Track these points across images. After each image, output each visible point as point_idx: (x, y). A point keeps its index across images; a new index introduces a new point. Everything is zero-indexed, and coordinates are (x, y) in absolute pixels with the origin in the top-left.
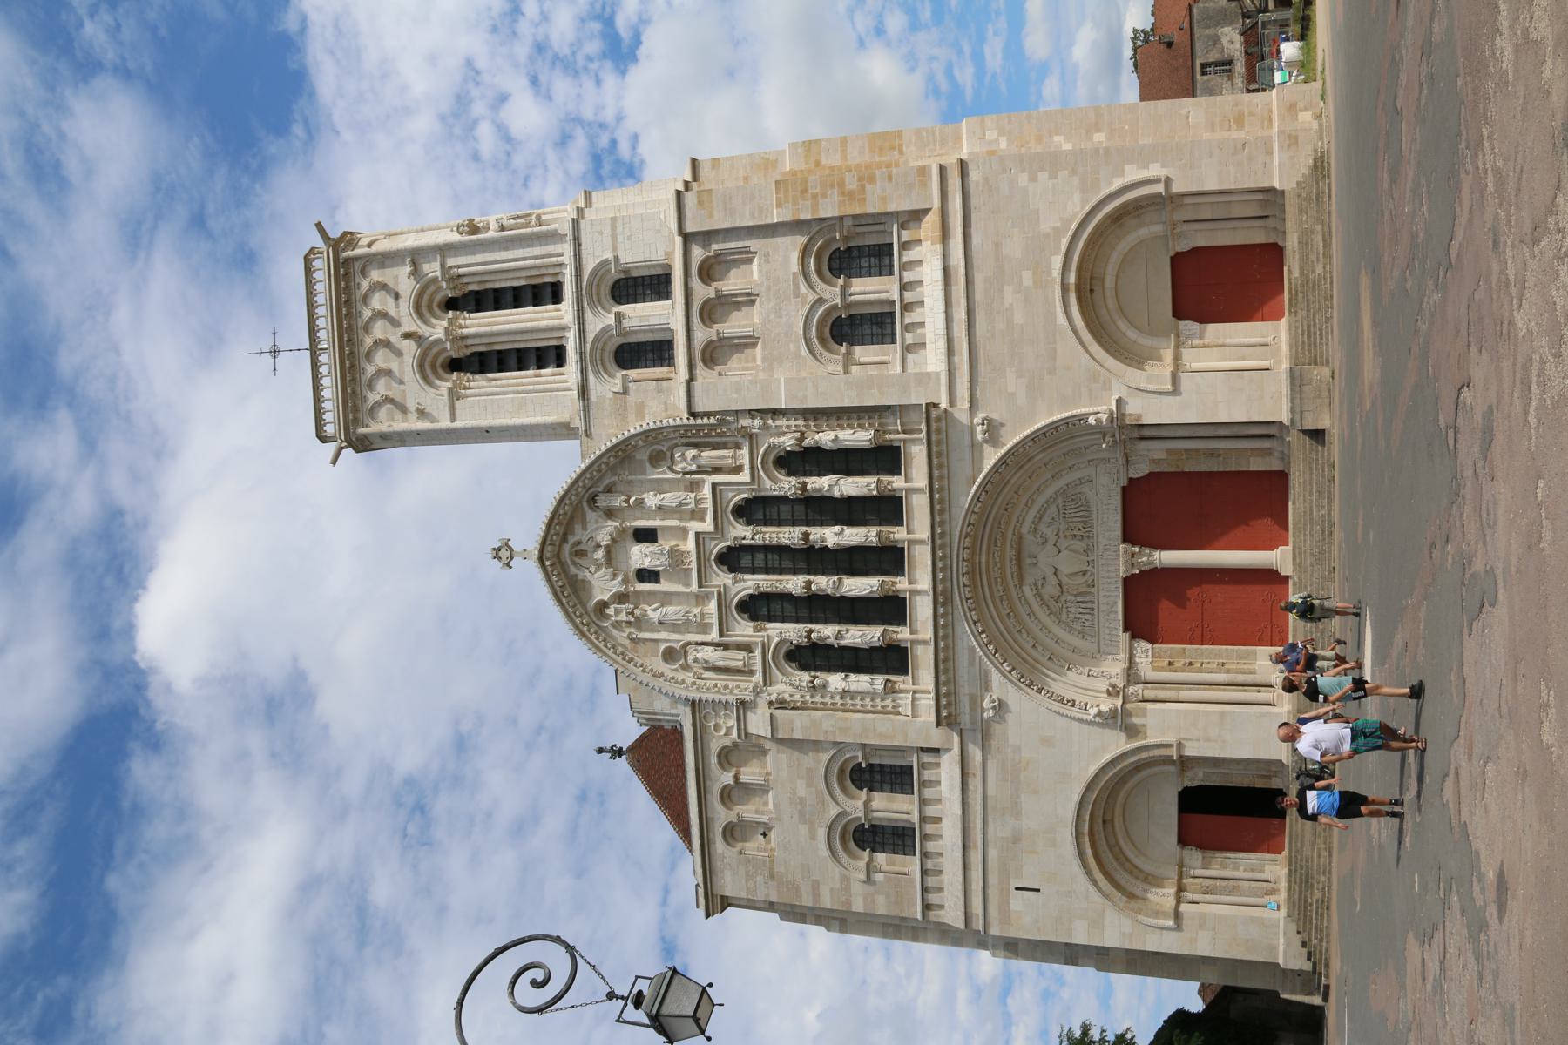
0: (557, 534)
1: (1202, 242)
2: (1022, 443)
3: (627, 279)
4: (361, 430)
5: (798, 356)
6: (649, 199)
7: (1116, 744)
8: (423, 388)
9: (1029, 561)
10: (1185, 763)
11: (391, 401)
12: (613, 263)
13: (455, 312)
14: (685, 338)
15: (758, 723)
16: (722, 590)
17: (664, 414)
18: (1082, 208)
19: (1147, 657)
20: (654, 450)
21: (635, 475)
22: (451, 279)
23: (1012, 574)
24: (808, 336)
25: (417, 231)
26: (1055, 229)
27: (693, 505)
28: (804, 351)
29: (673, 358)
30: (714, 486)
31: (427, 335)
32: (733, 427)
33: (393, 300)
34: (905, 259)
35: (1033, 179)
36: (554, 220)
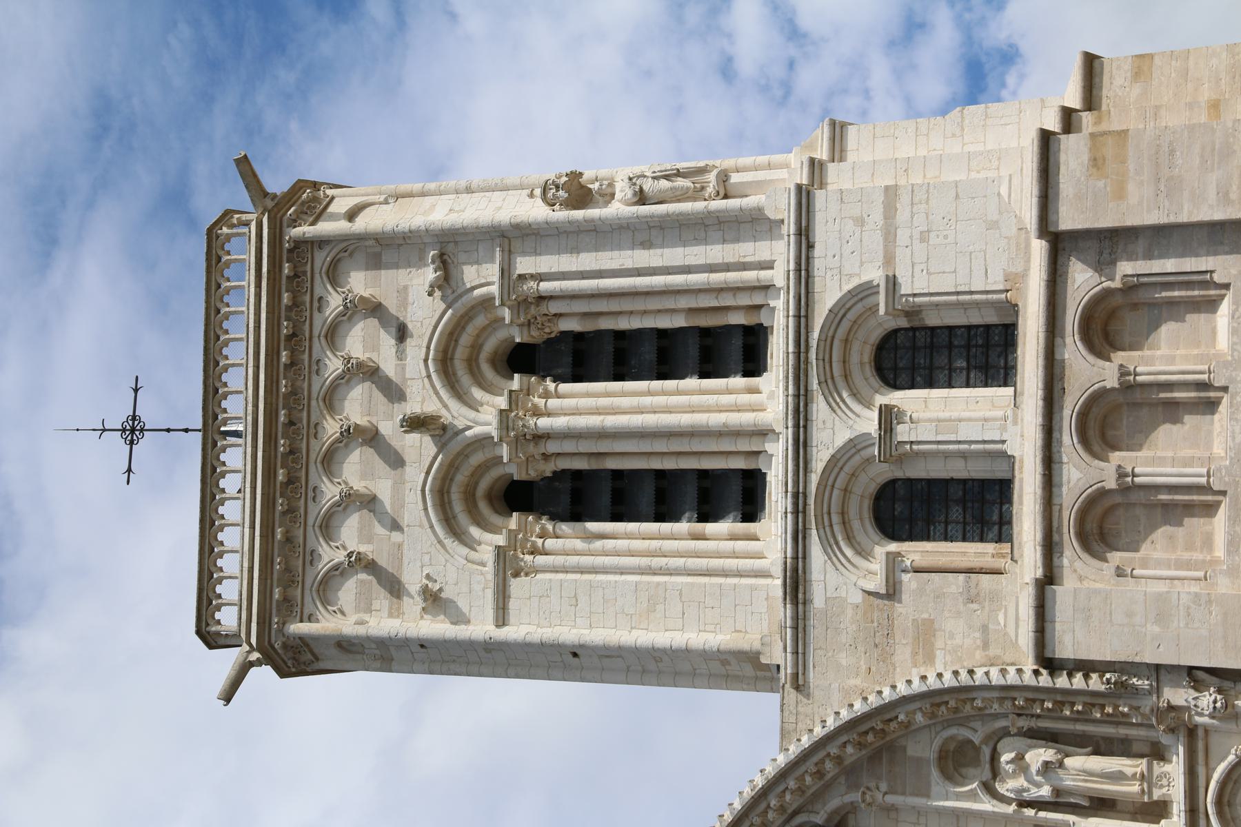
3: (913, 329)
4: (298, 628)
6: (980, 147)
8: (440, 542)
11: (371, 566)
12: (882, 298)
13: (525, 378)
14: (1039, 478)
17: (979, 655)
20: (952, 738)
21: (903, 794)
22: (522, 304)
25: (457, 192)
29: (1010, 523)
31: (460, 424)
32: (1147, 704)
33: (393, 342)
36: (758, 186)
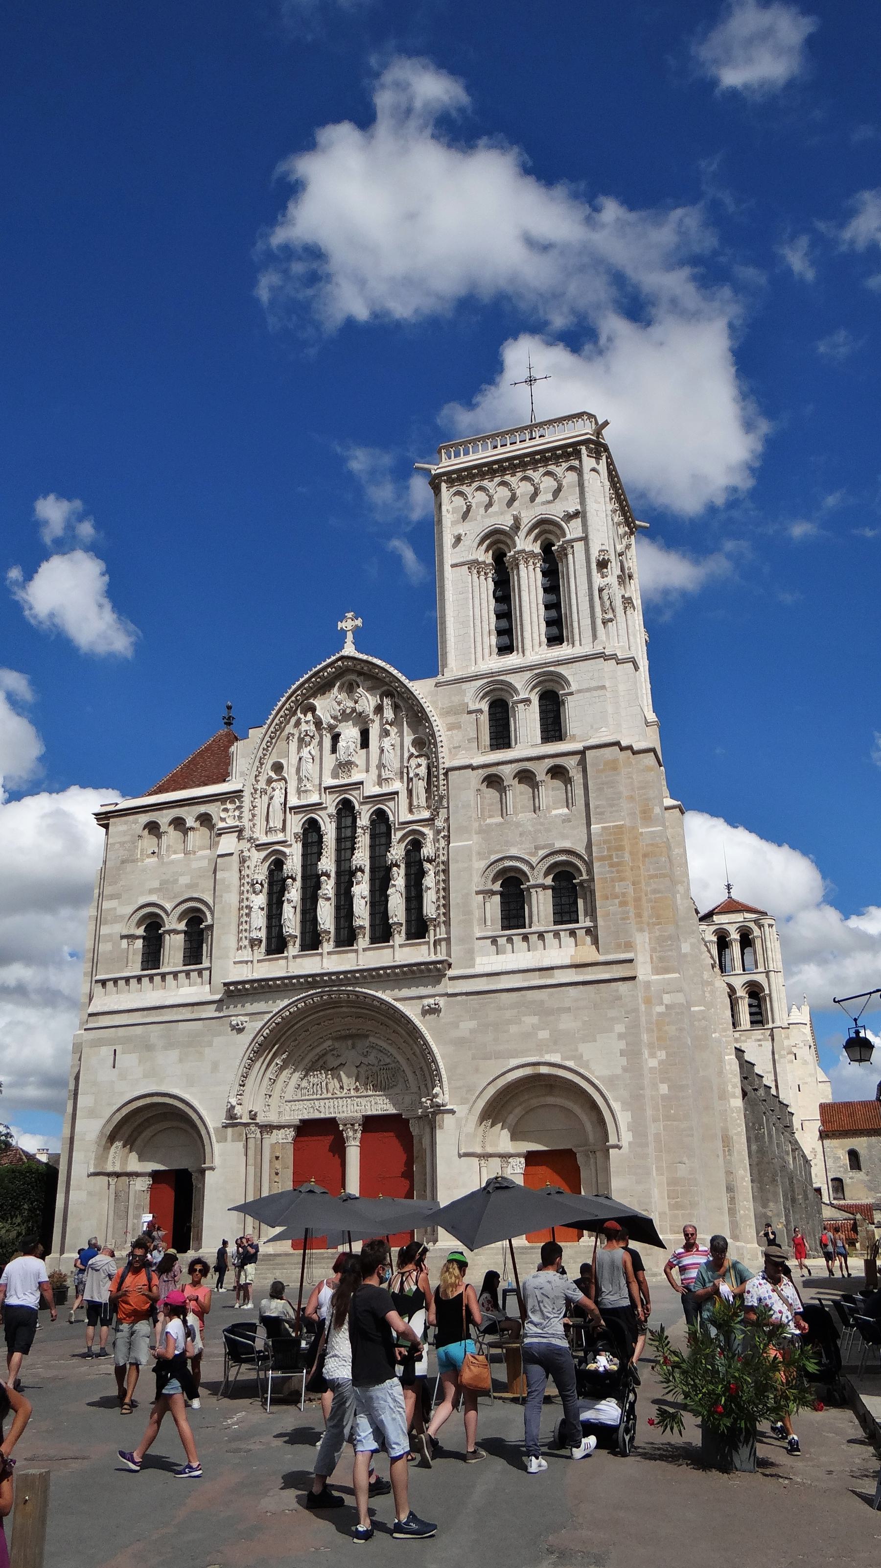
1: (583, 1174)
2: (422, 1037)
4: (444, 486)
5: (491, 853)
9: (350, 1042)
10: (202, 1172)
12: (566, 691)
15: (228, 843)
16: (324, 805)
18: (597, 1078)
23: (339, 1031)
26: (581, 1056)
28: (494, 857)
30: (397, 793)
35: (621, 1036)
36: (607, 634)
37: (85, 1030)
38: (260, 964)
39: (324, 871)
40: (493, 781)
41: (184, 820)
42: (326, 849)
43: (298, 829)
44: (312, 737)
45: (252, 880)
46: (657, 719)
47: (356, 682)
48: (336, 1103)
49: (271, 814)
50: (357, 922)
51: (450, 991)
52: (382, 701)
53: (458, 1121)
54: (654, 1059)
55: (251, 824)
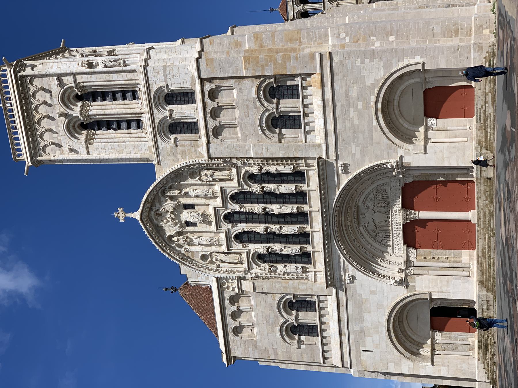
0: (148, 207)
1: (437, 85)
4: (39, 158)
5: (257, 135)
7: (402, 293)
8: (70, 138)
9: (361, 216)
10: (432, 300)
12: (165, 88)
15: (247, 286)
16: (227, 230)
19: (414, 255)
24: (261, 126)
27: (212, 195)
28: (260, 132)
30: (221, 188)
34: (304, 94)
36: (133, 63)
37: (351, 368)
38: (317, 268)
39: (264, 230)
40: (217, 132)
41: (233, 312)
42: (252, 229)
43: (240, 246)
44: (187, 237)
45: (269, 272)
46: (181, 39)
47: (155, 212)
48: (395, 224)
49: (231, 261)
50: (295, 211)
51: (334, 158)
52: (168, 196)
53: (406, 154)
54: (376, 43)
55: (236, 273)
